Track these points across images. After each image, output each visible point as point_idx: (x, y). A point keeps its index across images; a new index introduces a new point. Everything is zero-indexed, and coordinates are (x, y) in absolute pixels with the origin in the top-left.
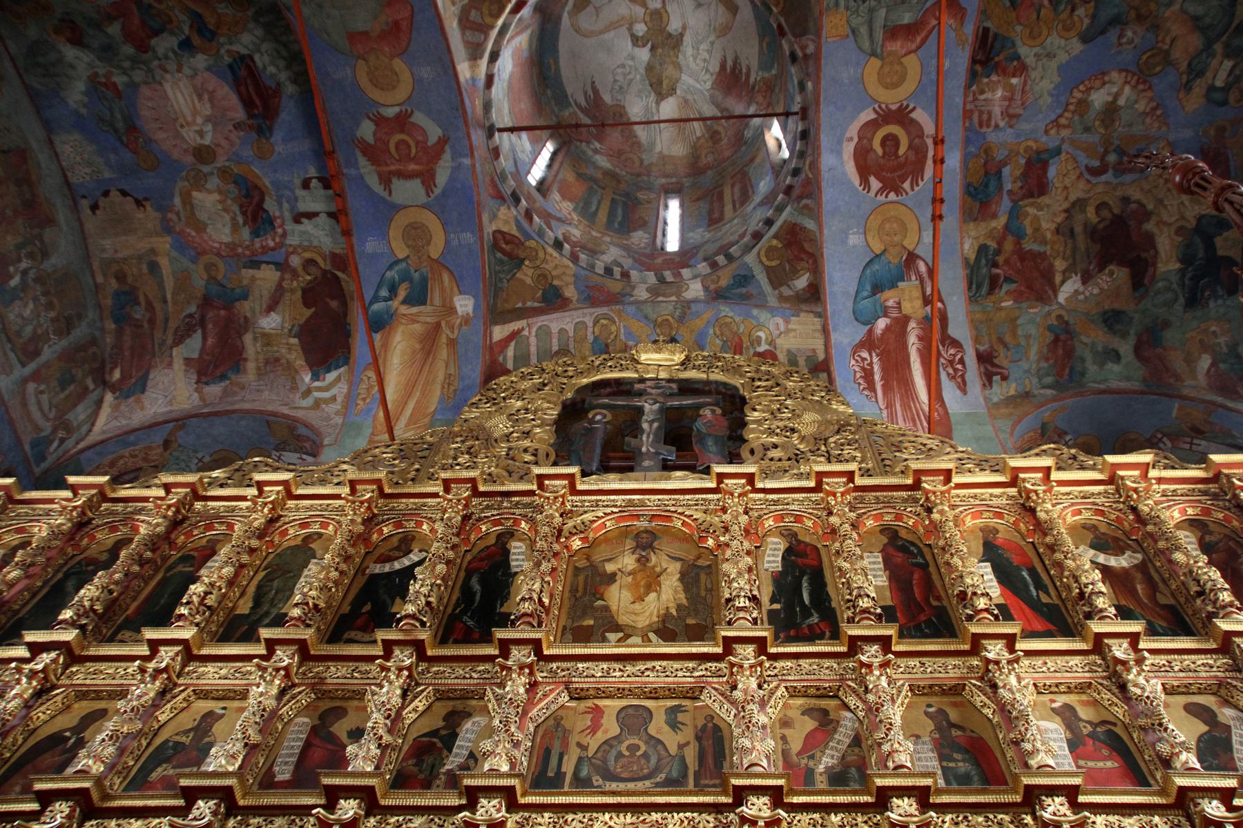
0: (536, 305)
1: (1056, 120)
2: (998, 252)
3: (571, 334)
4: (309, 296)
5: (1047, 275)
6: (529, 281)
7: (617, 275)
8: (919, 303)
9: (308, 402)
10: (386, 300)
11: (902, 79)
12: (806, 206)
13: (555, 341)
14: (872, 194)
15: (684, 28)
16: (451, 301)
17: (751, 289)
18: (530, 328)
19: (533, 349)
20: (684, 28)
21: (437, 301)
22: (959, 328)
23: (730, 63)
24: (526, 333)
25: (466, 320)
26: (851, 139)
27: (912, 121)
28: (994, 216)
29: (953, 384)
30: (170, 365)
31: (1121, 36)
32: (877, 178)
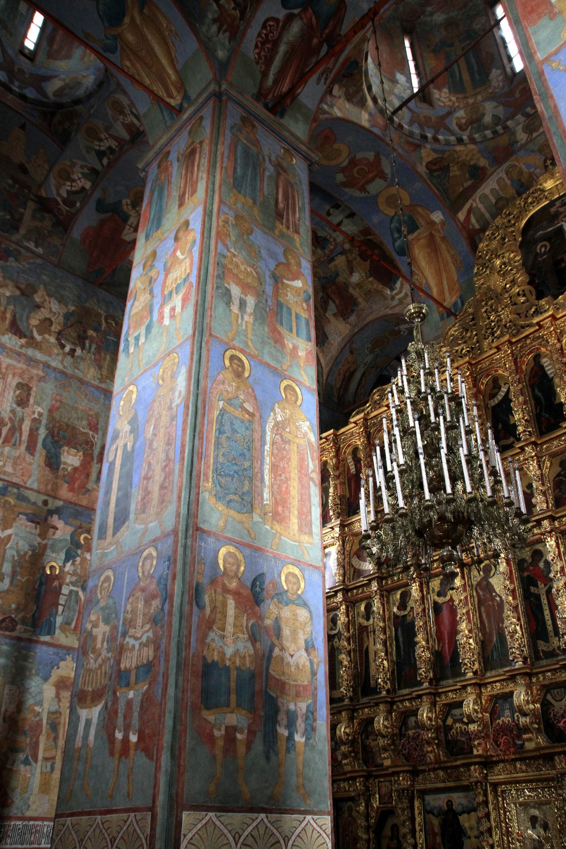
4: (364, 256)
6: (458, 173)
9: (395, 302)
10: (399, 238)
18: (475, 202)
21: (423, 223)
24: (474, 205)
25: (443, 223)
30: (329, 321)
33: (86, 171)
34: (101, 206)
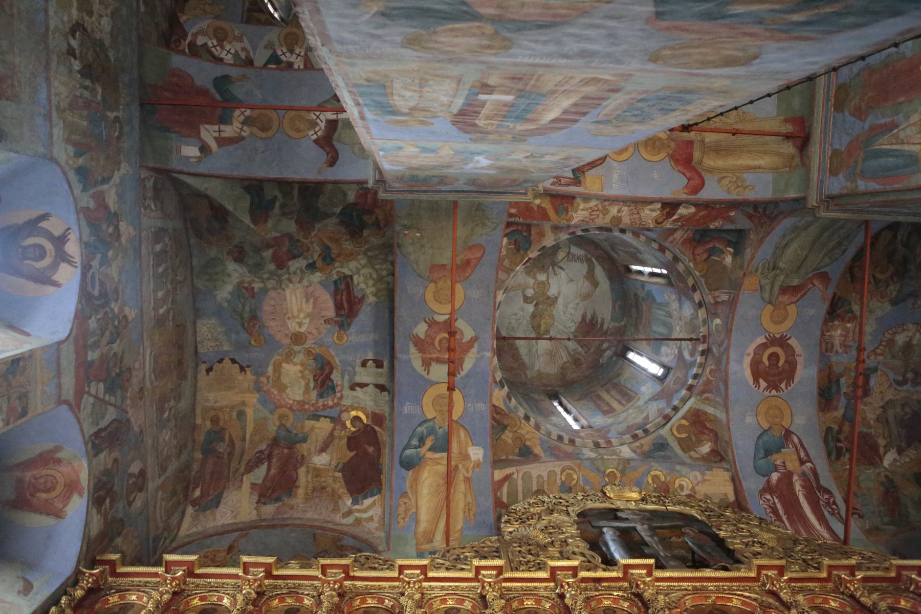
0: (515, 458)
1: (874, 350)
2: (840, 432)
3: (546, 479)
4: (353, 442)
5: (874, 448)
7: (566, 441)
8: (797, 463)
10: (416, 447)
11: (785, 318)
12: (707, 399)
13: (535, 483)
14: (761, 389)
15: (559, 293)
16: (466, 450)
17: (668, 453)
19: (520, 488)
20: (559, 293)
22: (827, 480)
23: (589, 317)
24: (515, 476)
25: (478, 464)
26: (749, 354)
27: (788, 345)
28: (836, 409)
29: (834, 518)
30: (240, 487)
31: (914, 304)
32: (764, 380)
33: (243, 55)
34: (222, 82)
